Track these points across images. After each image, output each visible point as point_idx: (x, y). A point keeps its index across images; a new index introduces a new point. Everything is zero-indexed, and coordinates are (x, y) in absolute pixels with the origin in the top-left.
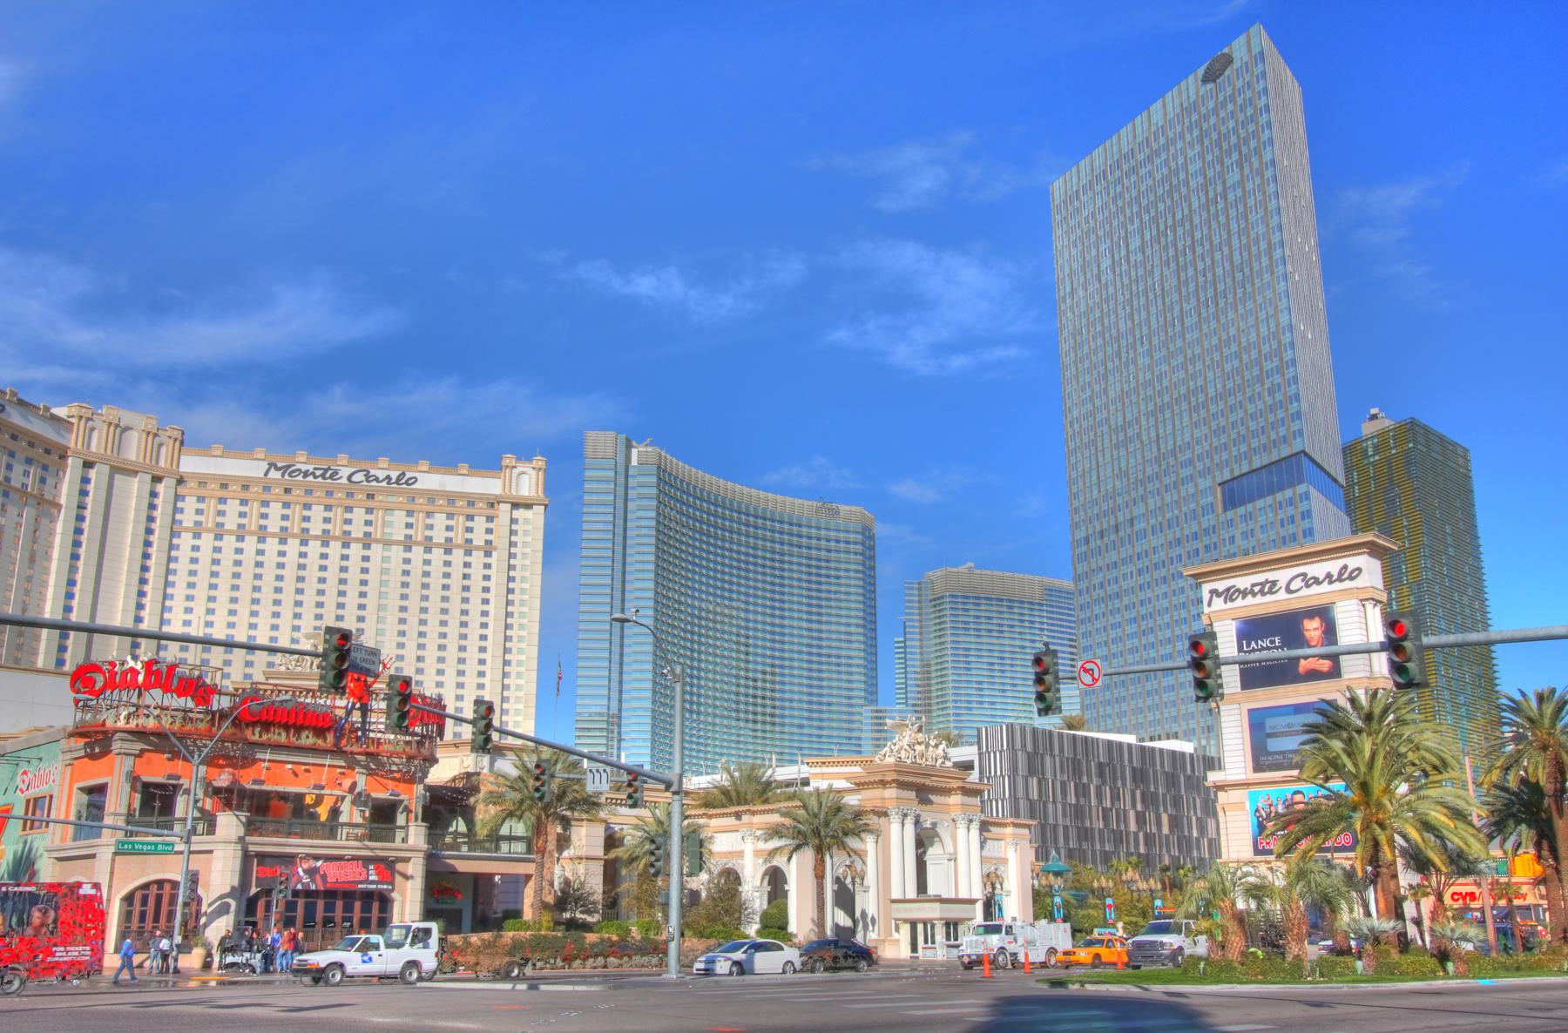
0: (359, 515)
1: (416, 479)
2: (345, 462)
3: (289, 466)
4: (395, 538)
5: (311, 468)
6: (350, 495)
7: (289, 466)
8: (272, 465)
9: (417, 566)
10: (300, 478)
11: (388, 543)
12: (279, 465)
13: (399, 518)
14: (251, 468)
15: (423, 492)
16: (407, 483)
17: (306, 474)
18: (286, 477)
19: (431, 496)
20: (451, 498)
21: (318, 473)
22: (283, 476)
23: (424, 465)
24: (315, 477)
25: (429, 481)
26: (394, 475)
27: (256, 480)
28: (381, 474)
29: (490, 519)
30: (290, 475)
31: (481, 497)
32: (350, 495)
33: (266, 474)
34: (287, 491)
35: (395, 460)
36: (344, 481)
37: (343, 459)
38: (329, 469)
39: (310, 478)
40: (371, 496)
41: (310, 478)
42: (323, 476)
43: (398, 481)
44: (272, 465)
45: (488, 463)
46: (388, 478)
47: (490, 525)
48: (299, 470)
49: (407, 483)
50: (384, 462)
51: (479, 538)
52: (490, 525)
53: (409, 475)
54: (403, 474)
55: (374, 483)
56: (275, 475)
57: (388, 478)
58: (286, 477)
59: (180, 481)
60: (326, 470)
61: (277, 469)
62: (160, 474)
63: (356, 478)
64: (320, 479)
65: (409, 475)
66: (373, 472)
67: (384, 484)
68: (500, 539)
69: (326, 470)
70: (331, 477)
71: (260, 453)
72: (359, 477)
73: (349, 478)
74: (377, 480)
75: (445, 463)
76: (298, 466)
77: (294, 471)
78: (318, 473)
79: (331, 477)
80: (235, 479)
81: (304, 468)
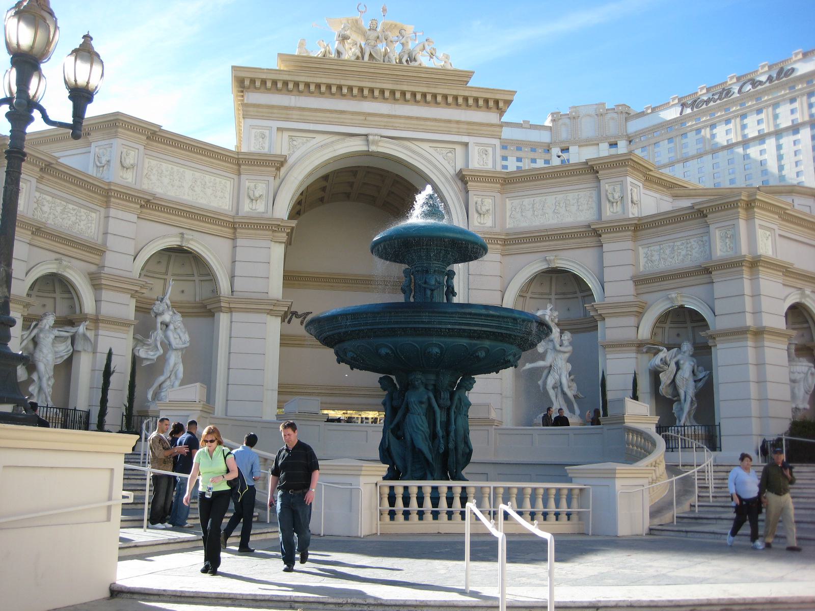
7: (695, 101)
10: (704, 106)
17: (707, 102)
18: (695, 110)
21: (716, 97)
24: (715, 102)
30: (696, 108)
33: (681, 114)
36: (736, 95)
39: (712, 104)
42: (720, 98)
53: (785, 70)
56: (688, 111)
62: (613, 140)
67: (767, 84)
69: (721, 93)
72: (749, 87)
73: (740, 91)
74: (761, 83)
78: (716, 97)
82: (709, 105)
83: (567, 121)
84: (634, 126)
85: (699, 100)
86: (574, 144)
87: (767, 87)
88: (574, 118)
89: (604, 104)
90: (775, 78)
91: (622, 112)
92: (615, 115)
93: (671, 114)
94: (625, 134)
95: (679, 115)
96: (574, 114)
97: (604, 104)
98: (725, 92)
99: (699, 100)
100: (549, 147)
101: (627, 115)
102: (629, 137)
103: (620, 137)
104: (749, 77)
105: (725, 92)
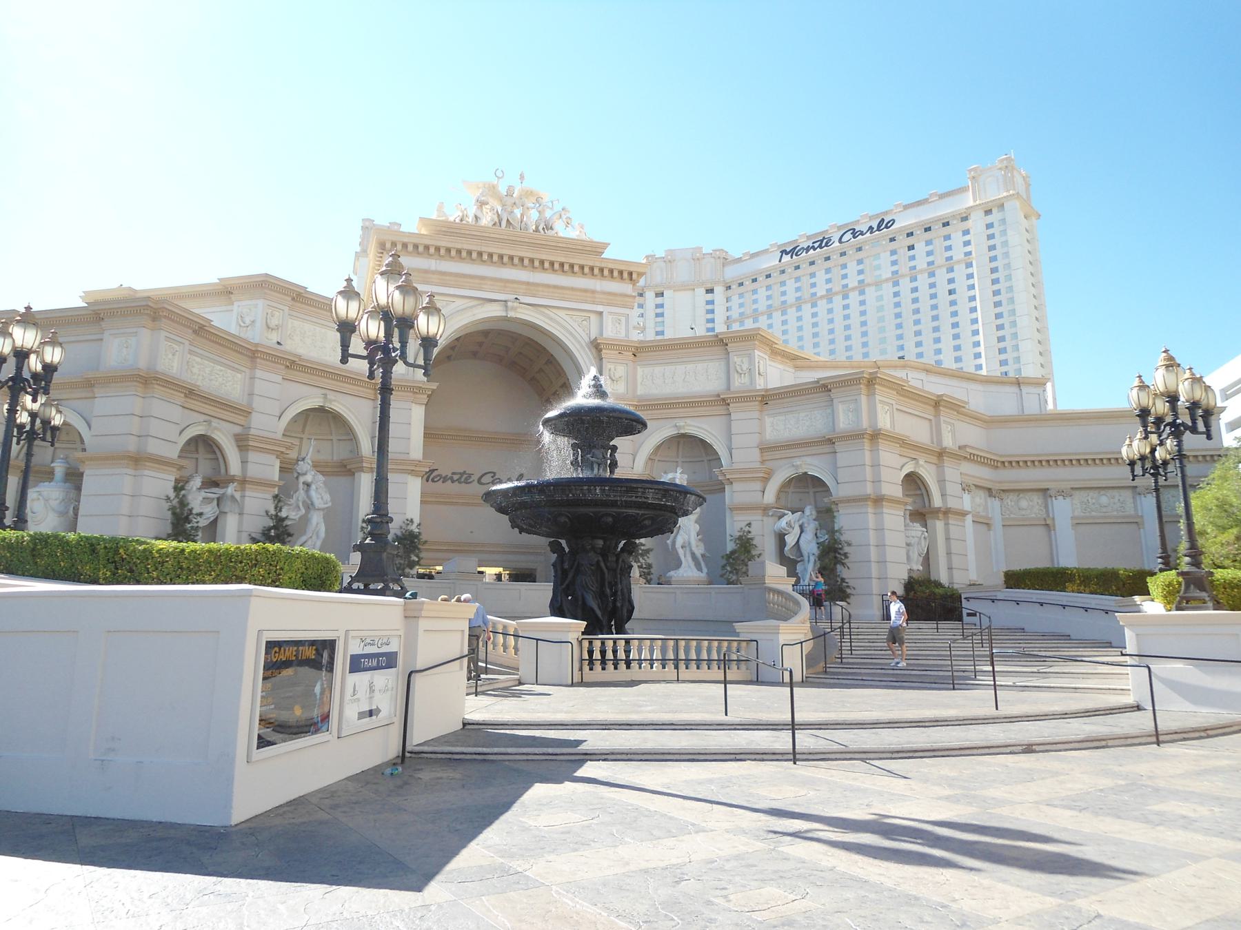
0: (852, 268)
1: (894, 221)
4: (884, 277)
7: (795, 248)
9: (906, 296)
10: (804, 254)
11: (878, 284)
13: (886, 258)
15: (900, 230)
17: (808, 249)
22: (792, 258)
24: (815, 249)
30: (796, 255)
33: (780, 261)
34: (797, 268)
36: (837, 244)
38: (824, 238)
39: (812, 251)
41: (812, 251)
42: (820, 247)
43: (878, 230)
44: (782, 252)
46: (871, 228)
48: (803, 248)
49: (887, 227)
54: (883, 220)
55: (860, 237)
56: (786, 258)
57: (871, 228)
58: (794, 256)
60: (822, 241)
61: (787, 253)
63: (843, 240)
64: (818, 250)
67: (868, 233)
69: (822, 241)
70: (826, 245)
72: (848, 236)
77: (799, 250)
78: (816, 245)
82: (809, 253)
83: (663, 264)
84: (731, 273)
85: (798, 248)
86: (669, 288)
87: (867, 237)
88: (670, 261)
89: (701, 248)
90: (875, 229)
91: (719, 258)
92: (713, 260)
93: (772, 262)
94: (722, 279)
96: (669, 257)
97: (701, 248)
98: (825, 241)
99: (798, 248)
100: (643, 290)
101: (724, 260)
104: (851, 228)
105: (825, 241)
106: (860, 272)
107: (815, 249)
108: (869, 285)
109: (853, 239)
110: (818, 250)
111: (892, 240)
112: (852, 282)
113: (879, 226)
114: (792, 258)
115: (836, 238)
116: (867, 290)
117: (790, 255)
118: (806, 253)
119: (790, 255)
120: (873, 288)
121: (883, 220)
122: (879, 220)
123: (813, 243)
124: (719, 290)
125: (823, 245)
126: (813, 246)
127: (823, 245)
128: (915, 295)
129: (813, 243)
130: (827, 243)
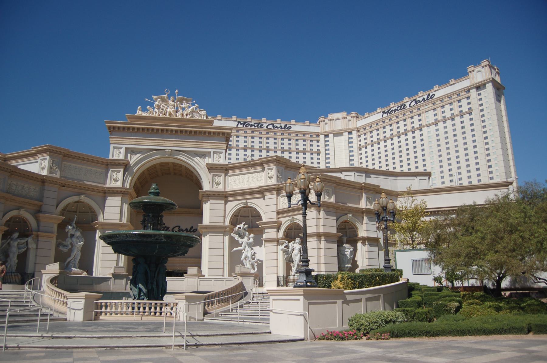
1: (434, 95)
2: (407, 100)
3: (389, 110)
4: (431, 122)
5: (396, 108)
6: (411, 112)
7: (389, 110)
8: (384, 112)
10: (393, 113)
12: (386, 111)
14: (377, 116)
16: (431, 98)
17: (395, 111)
18: (389, 115)
19: (441, 99)
20: (449, 96)
21: (399, 108)
22: (388, 115)
23: (436, 88)
24: (398, 110)
25: (440, 92)
26: (425, 97)
27: (379, 120)
28: (421, 99)
29: (468, 98)
30: (390, 114)
31: (462, 90)
32: (411, 112)
33: (382, 117)
34: (390, 120)
35: (424, 91)
36: (408, 107)
37: (406, 99)
38: (402, 105)
39: (397, 112)
40: (419, 109)
42: (401, 109)
43: (427, 99)
45: (463, 74)
46: (424, 99)
47: (469, 101)
48: (393, 110)
49: (431, 98)
50: (421, 94)
51: (465, 109)
52: (469, 101)
53: (431, 95)
54: (429, 95)
55: (419, 103)
56: (385, 115)
57: (424, 99)
58: (389, 115)
59: (358, 131)
60: (401, 106)
61: (385, 113)
63: (411, 105)
64: (400, 111)
65: (431, 95)
66: (417, 100)
67: (423, 102)
68: (475, 106)
69: (401, 106)
71: (379, 110)
72: (413, 103)
73: (410, 106)
74: (420, 102)
75: (444, 82)
76: (392, 109)
78: (399, 108)
79: (403, 108)
80: (373, 123)
81: (394, 109)
95: (381, 117)
98: (403, 106)
102: (358, 129)
103: (354, 129)
105: (403, 106)
106: (420, 120)
107: (398, 110)
108: (424, 126)
109: (415, 105)
110: (400, 111)
111: (434, 104)
112: (416, 125)
113: (428, 97)
114: (388, 115)
115: (407, 104)
116: (423, 129)
117: (387, 114)
118: (394, 112)
119: (387, 114)
120: (426, 128)
121: (429, 95)
122: (427, 95)
123: (398, 107)
124: (354, 132)
125: (402, 108)
126: (397, 109)
127: (402, 108)
128: (446, 130)
129: (398, 107)
130: (404, 107)
